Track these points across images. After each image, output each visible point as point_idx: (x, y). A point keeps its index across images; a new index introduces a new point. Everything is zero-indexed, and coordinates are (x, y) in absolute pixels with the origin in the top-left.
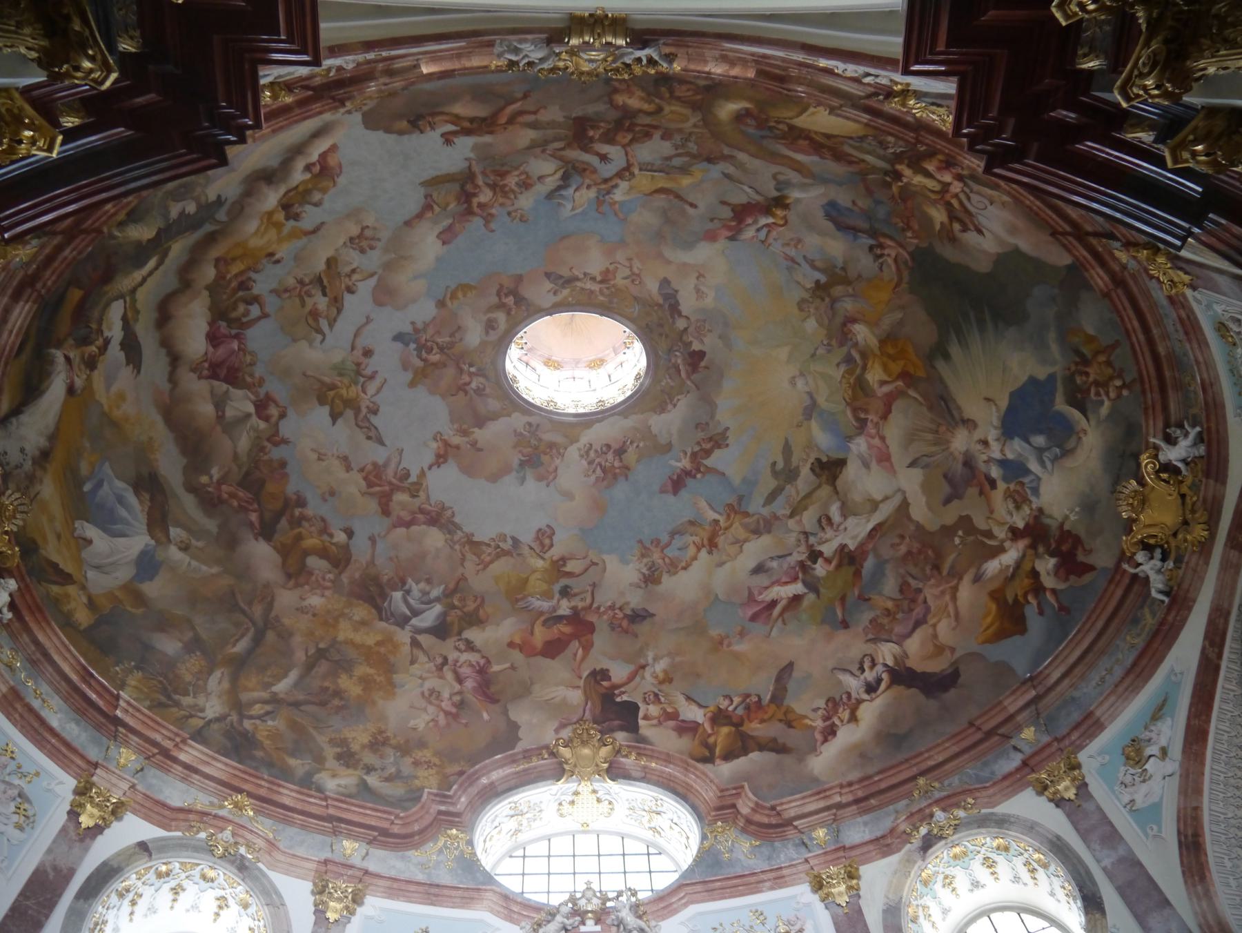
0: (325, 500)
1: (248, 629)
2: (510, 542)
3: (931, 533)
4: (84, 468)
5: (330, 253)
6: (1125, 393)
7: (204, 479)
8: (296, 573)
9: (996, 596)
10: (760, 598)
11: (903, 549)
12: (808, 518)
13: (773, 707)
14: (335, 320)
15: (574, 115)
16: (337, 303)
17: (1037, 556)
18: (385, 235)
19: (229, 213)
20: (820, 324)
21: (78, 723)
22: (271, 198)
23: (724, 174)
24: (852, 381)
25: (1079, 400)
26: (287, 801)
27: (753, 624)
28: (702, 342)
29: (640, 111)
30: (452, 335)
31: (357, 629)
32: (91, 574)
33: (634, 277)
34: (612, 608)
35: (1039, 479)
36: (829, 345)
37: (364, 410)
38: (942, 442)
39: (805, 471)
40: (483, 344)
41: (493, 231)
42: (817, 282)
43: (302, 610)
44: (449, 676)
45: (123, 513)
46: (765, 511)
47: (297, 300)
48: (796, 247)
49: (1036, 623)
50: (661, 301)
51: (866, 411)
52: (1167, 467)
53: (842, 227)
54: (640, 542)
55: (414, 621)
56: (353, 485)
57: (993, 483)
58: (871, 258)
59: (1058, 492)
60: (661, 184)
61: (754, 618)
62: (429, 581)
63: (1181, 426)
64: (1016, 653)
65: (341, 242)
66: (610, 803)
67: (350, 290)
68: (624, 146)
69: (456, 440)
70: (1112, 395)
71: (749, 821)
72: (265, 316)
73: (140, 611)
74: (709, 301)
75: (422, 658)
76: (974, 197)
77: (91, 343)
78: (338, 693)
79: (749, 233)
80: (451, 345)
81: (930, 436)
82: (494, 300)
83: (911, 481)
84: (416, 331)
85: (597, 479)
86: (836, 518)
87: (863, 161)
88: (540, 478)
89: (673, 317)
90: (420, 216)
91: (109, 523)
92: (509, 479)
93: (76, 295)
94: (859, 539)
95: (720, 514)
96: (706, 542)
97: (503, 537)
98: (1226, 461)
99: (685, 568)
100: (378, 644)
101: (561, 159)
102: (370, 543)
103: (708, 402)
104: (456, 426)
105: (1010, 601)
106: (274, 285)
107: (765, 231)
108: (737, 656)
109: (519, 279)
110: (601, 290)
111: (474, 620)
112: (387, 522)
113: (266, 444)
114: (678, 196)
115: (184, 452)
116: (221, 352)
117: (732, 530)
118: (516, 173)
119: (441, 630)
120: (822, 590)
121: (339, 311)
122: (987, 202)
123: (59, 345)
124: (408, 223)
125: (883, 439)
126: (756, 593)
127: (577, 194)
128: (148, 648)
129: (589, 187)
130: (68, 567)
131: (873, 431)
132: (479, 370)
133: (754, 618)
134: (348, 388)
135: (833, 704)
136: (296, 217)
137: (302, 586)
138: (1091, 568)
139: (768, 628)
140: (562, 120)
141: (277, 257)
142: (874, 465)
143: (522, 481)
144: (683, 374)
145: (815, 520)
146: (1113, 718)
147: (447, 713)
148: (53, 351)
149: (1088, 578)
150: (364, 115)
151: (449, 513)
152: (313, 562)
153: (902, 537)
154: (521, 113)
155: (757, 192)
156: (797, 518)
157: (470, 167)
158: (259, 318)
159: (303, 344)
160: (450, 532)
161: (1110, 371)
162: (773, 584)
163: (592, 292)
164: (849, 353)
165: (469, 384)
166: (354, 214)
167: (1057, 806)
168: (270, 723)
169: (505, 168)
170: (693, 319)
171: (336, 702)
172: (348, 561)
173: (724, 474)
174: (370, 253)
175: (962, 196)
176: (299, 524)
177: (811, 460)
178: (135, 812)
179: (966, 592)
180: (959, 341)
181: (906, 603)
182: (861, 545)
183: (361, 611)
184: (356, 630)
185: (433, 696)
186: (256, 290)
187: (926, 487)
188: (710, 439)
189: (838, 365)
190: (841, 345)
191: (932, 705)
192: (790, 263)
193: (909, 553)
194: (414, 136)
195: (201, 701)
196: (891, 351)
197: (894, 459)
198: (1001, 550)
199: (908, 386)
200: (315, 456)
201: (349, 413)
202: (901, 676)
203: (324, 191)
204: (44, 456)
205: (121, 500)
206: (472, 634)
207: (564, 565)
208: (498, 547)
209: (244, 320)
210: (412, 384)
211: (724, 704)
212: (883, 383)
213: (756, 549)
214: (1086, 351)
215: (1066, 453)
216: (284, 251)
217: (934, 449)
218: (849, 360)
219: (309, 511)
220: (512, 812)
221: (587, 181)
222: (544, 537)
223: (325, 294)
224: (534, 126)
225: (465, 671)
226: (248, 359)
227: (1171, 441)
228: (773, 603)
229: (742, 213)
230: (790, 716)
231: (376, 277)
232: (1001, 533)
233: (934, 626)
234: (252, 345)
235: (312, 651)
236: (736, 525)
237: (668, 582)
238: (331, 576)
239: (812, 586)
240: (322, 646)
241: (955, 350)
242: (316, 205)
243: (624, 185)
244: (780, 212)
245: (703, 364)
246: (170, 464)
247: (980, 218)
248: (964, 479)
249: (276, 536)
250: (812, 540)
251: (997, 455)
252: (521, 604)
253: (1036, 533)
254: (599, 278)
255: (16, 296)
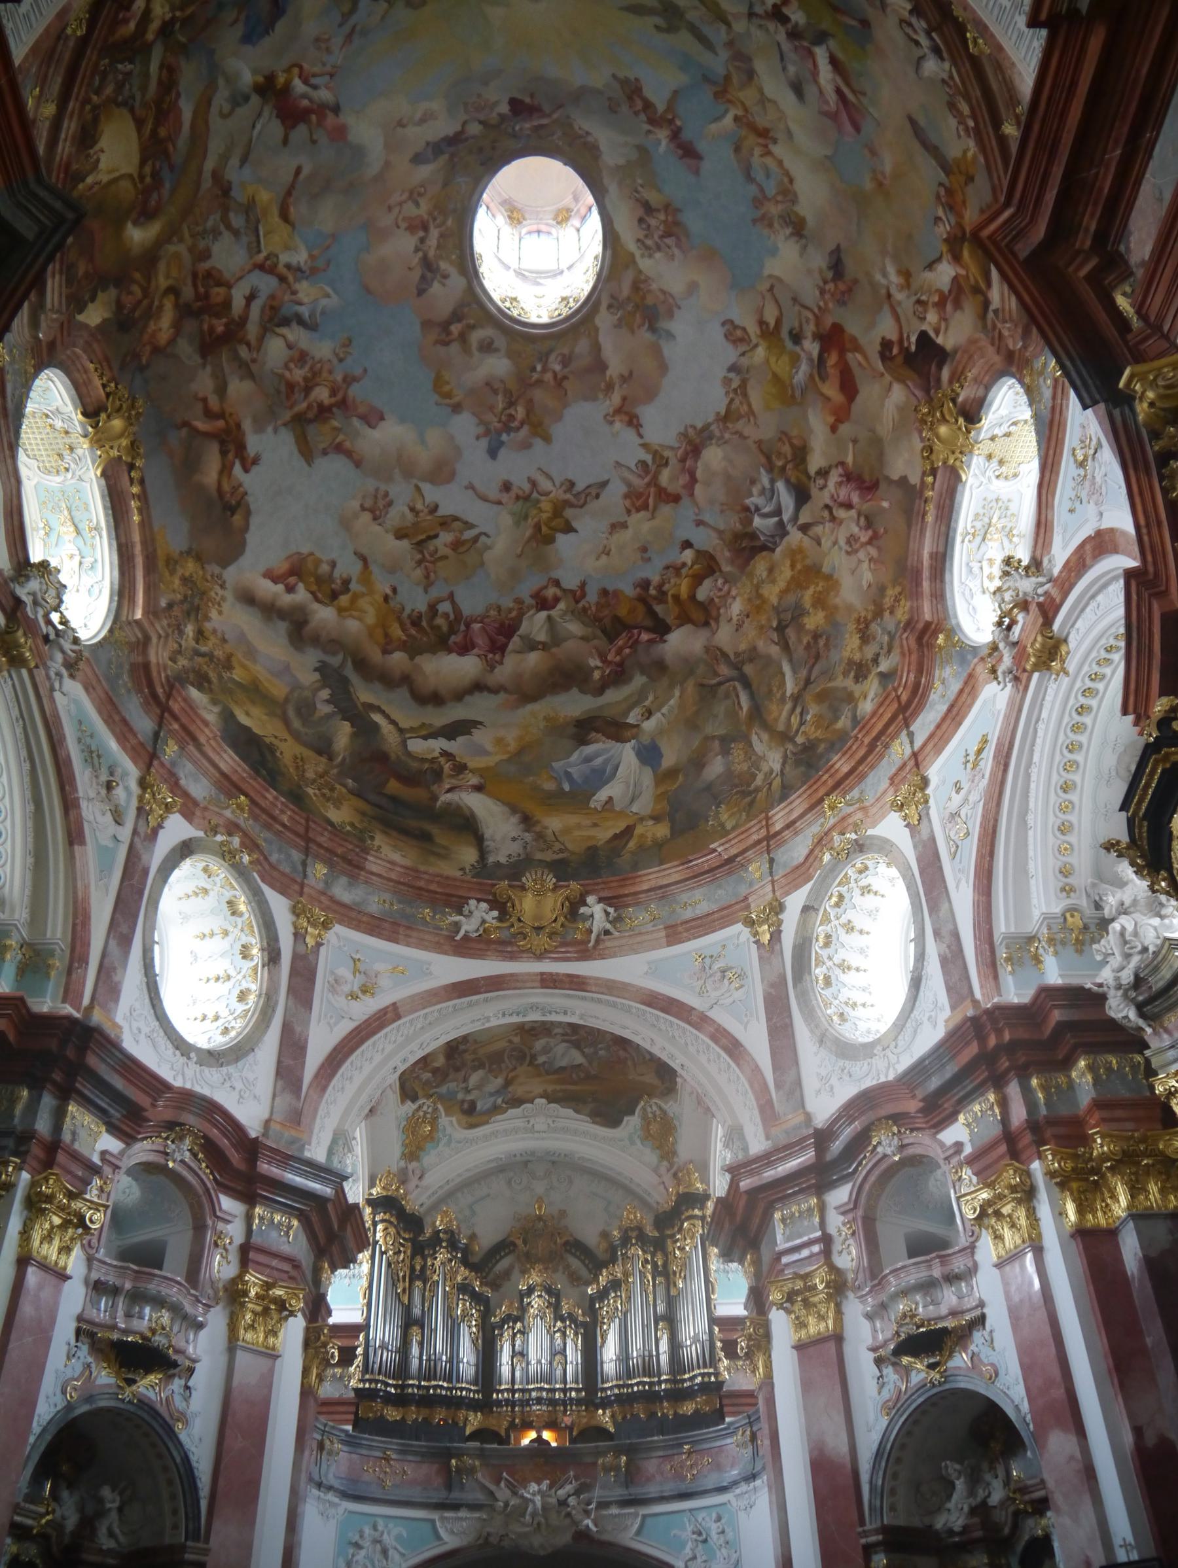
0: (649, 559)
1: (735, 688)
2: (732, 375)
4: (549, 786)
5: (390, 537)
7: (597, 675)
8: (704, 615)
14: (466, 523)
15: (200, 361)
16: (446, 523)
18: (371, 484)
19: (334, 654)
21: (720, 887)
22: (324, 615)
23: (241, 166)
26: (845, 769)
28: (496, 103)
29: (177, 305)
30: (496, 392)
31: (773, 578)
32: (635, 809)
33: (414, 196)
34: (822, 292)
37: (568, 496)
40: (510, 355)
41: (365, 370)
43: (739, 626)
44: (841, 513)
45: (599, 761)
46: (724, 54)
47: (440, 564)
48: (328, 40)
50: (446, 156)
54: (754, 221)
55: (786, 517)
56: (641, 525)
60: (275, 219)
61: (857, 129)
62: (753, 482)
65: (377, 528)
66: (1015, 424)
67: (435, 508)
68: (229, 286)
69: (616, 398)
72: (451, 597)
73: (681, 778)
74: (436, 105)
75: (818, 530)
77: (442, 769)
78: (816, 636)
79: (324, 95)
80: (508, 393)
82: (455, 348)
84: (487, 433)
85: (678, 246)
88: (670, 315)
89: (467, 139)
90: (349, 454)
91: (602, 777)
92: (668, 350)
93: (393, 786)
95: (726, 111)
96: (761, 141)
97: (727, 381)
99: (791, 181)
100: (793, 567)
101: (261, 339)
102: (701, 528)
103: (580, 96)
104: (601, 396)
106: (420, 590)
109: (426, 324)
110: (439, 226)
111: (801, 454)
112: (686, 501)
113: (580, 605)
114: (289, 193)
115: (566, 688)
116: (481, 641)
117: (748, 103)
118: (287, 374)
119: (802, 496)
121: (456, 519)
123: (435, 798)
124: (358, 464)
126: (825, 108)
127: (306, 300)
128: (709, 788)
129: (294, 293)
130: (621, 826)
132: (540, 360)
133: (857, 129)
134: (541, 510)
136: (346, 582)
137: (719, 615)
140: (209, 369)
141: (389, 591)
143: (670, 336)
144: (545, 121)
147: (870, 542)
148: (439, 803)
150: (225, 563)
151: (690, 430)
152: (702, 594)
154: (209, 414)
155: (259, 115)
156: (730, 18)
157: (285, 425)
158: (453, 603)
159: (488, 556)
160: (711, 438)
162: (816, 82)
163: (442, 236)
165: (555, 374)
166: (346, 524)
168: (809, 717)
169: (283, 388)
170: (465, 117)
171: (821, 642)
172: (712, 558)
173: (675, 92)
174: (392, 495)
176: (664, 593)
178: (788, 893)
183: (760, 566)
184: (773, 582)
185: (851, 540)
186: (422, 607)
188: (630, 98)
194: (250, 499)
195: (765, 768)
200: (604, 557)
201: (569, 513)
203: (318, 562)
204: (527, 821)
205: (588, 760)
206: (815, 462)
207: (767, 324)
208: (735, 390)
209: (452, 617)
210: (547, 439)
213: (772, 83)
216: (383, 586)
219: (656, 579)
220: (979, 539)
221: (287, 297)
222: (734, 334)
223: (436, 536)
224: (221, 390)
225: (843, 493)
226: (493, 613)
228: (838, 91)
229: (292, 114)
231: (421, 485)
234: (479, 610)
235: (775, 636)
236: (741, 95)
237: (805, 209)
238: (720, 581)
240: (775, 624)
242: (333, 564)
243: (284, 258)
244: (281, 79)
245: (528, 100)
246: (573, 705)
249: (670, 620)
250: (759, 9)
252: (798, 393)
254: (421, 234)
255: (361, 868)
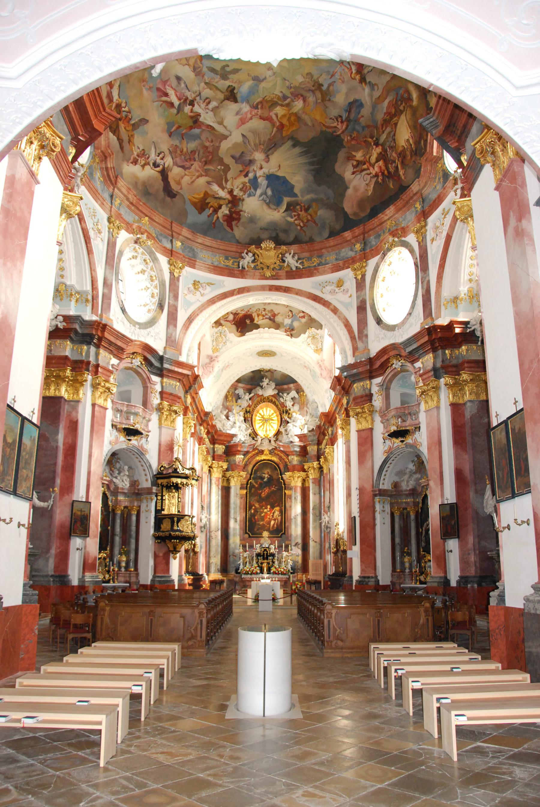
3: (218, 155)
6: (299, 227)
9: (206, 195)
10: (167, 87)
11: (207, 144)
12: (207, 92)
13: (130, 128)
17: (227, 205)
20: (301, 83)
24: (275, 100)
25: (290, 208)
27: (155, 90)
35: (254, 195)
36: (291, 88)
38: (256, 148)
39: (228, 83)
42: (322, 85)
46: (205, 69)
49: (204, 217)
51: (262, 108)
52: (283, 255)
53: (351, 105)
57: (246, 175)
58: (336, 115)
59: (252, 205)
63: (299, 259)
64: (193, 216)
70: (296, 222)
71: (107, 169)
76: (369, 177)
81: (257, 142)
83: (236, 137)
86: (211, 106)
87: (383, 132)
94: (205, 121)
98: (294, 278)
105: (207, 201)
107: (349, 67)
108: (141, 93)
120: (179, 115)
122: (367, 182)
125: (251, 119)
126: (168, 83)
131: (253, 113)
133: (158, 89)
135: (143, 154)
138: (232, 230)
139: (156, 99)
142: (238, 117)
145: (208, 96)
146: (199, 269)
149: (228, 229)
153: (212, 141)
155: (368, 72)
161: (305, 221)
162: (174, 89)
164: (288, 98)
167: (170, 273)
175: (368, 172)
177: (234, 85)
179: (202, 180)
180: (302, 152)
181: (188, 157)
182: (203, 123)
187: (236, 145)
189: (281, 92)
190: (292, 94)
191: (162, 194)
192: (331, 73)
193: (207, 148)
196: (292, 118)
197: (243, 126)
198: (223, 188)
199: (277, 128)
202: (164, 174)
211: (123, 105)
212: (277, 115)
214: (310, 211)
215: (268, 204)
217: (252, 144)
218: (285, 98)
227: (293, 257)
228: (166, 95)
230: (132, 139)
232: (229, 186)
233: (186, 175)
239: (180, 109)
241: (297, 150)
244: (358, 77)
247: (359, 176)
248: (245, 162)
250: (198, 98)
251: (258, 175)
253: (235, 201)
